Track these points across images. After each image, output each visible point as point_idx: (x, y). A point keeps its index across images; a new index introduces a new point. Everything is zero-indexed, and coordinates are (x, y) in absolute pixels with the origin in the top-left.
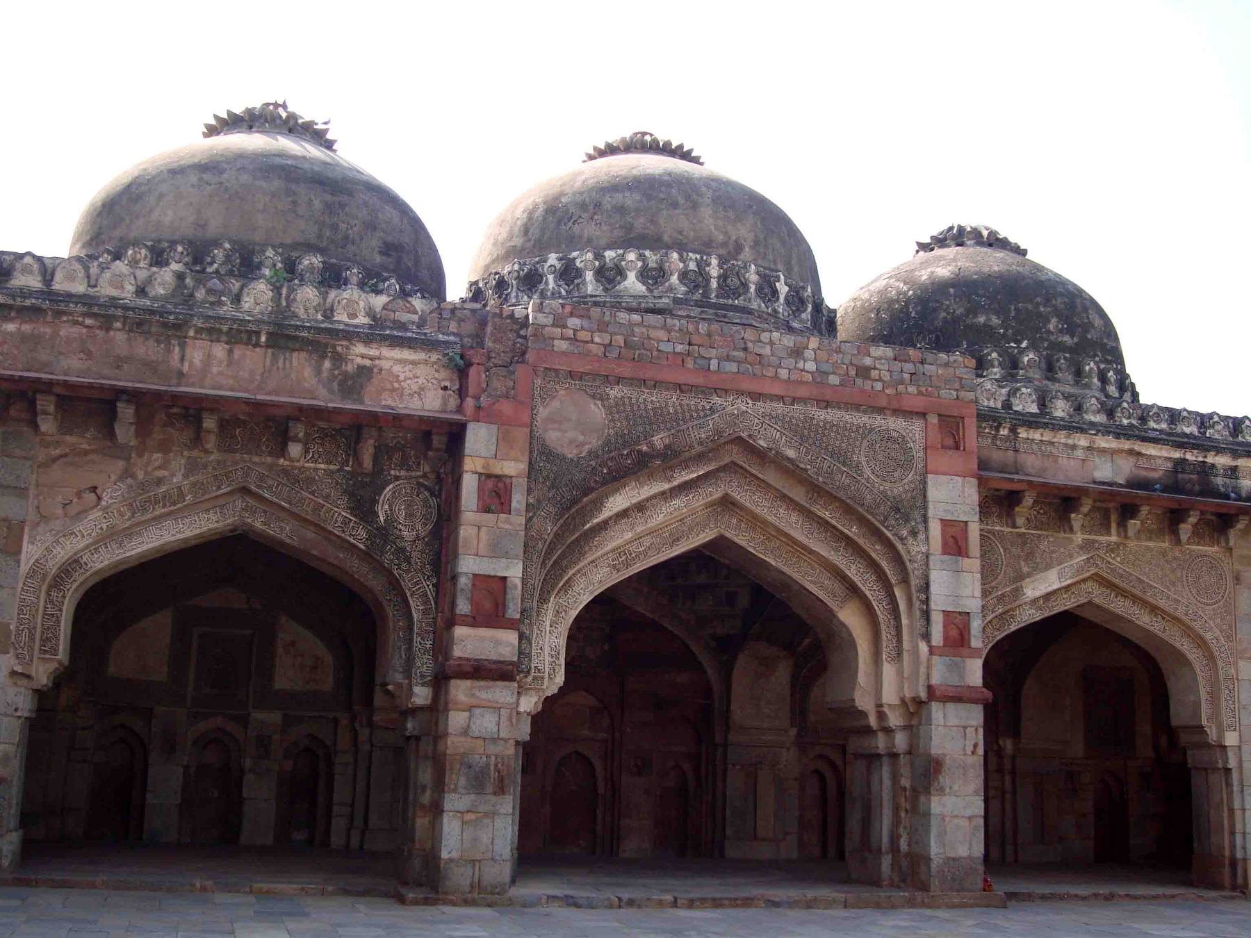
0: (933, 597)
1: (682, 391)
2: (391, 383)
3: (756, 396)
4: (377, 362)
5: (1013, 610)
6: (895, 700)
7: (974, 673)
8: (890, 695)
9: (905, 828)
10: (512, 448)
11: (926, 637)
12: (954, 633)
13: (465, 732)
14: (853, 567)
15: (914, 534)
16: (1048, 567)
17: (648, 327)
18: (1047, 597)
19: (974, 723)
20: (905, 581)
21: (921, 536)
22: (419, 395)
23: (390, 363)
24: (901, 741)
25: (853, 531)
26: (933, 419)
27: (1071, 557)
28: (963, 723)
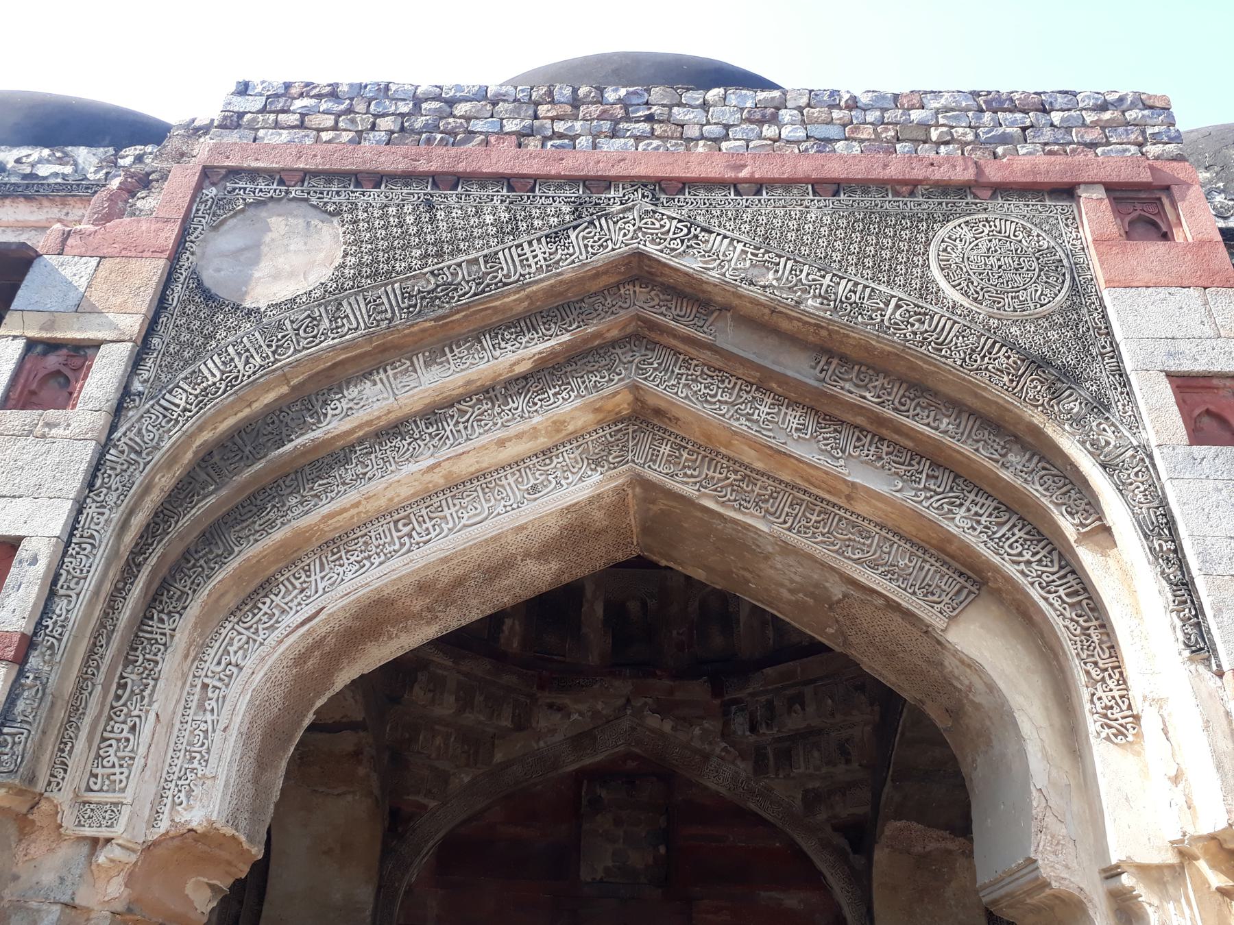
1: (511, 189)
15: (1100, 406)
17: (451, 102)
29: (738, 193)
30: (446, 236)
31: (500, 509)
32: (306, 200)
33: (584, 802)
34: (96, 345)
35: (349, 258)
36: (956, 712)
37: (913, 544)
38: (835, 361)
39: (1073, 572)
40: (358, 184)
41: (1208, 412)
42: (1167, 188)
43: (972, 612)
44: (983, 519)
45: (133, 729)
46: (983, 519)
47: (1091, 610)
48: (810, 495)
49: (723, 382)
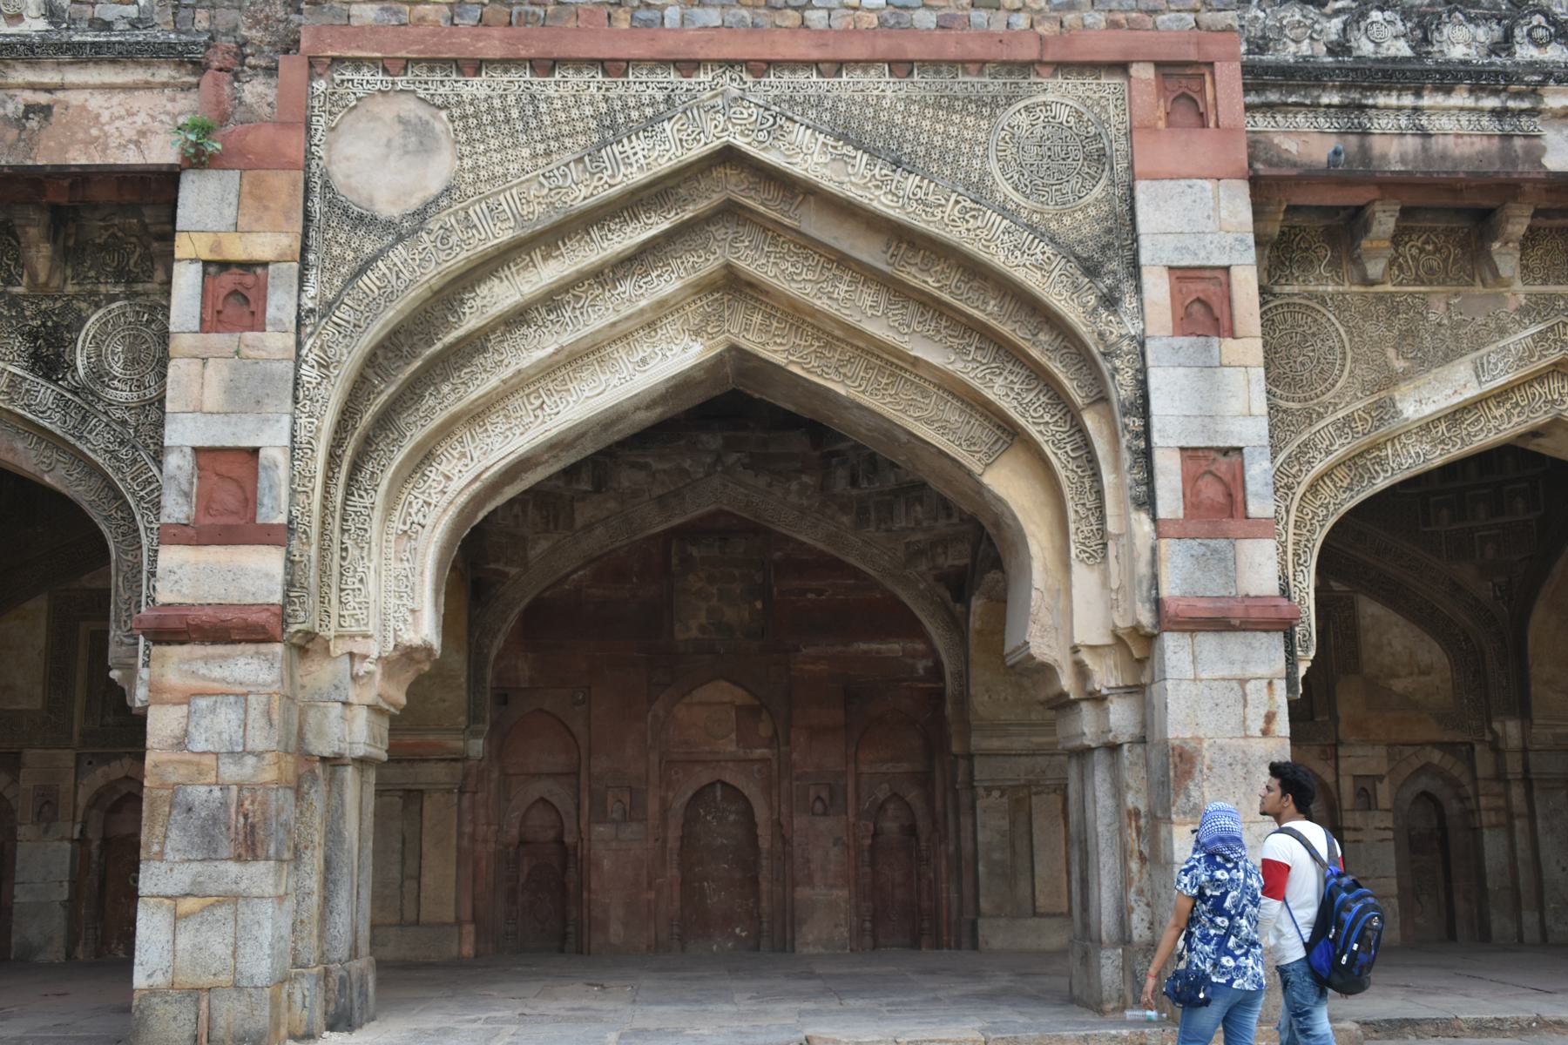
0: (1156, 422)
1: (606, 73)
2: (87, 132)
3: (761, 67)
4: (60, 95)
5: (1376, 446)
6: (1099, 637)
7: (1261, 568)
8: (1090, 626)
9: (1140, 892)
10: (266, 208)
11: (1147, 502)
12: (1211, 491)
13: (181, 743)
14: (1000, 381)
15: (1110, 301)
16: (1448, 357)
18: (1456, 415)
19: (1263, 671)
20: (1101, 399)
21: (1129, 303)
22: (137, 143)
23: (86, 94)
24: (1121, 717)
25: (986, 311)
26: (1144, 73)
27: (1502, 331)
28: (1237, 671)
29: (820, 73)
30: (551, 132)
31: (616, 381)
32: (414, 92)
33: (675, 561)
34: (265, 264)
35: (466, 160)
36: (998, 523)
37: (963, 401)
38: (904, 246)
39: (1080, 431)
40: (460, 72)
41: (1198, 300)
42: (1211, 64)
43: (1004, 458)
44: (1016, 387)
45: (361, 581)
46: (1016, 387)
47: (1090, 462)
48: (882, 359)
49: (806, 259)
